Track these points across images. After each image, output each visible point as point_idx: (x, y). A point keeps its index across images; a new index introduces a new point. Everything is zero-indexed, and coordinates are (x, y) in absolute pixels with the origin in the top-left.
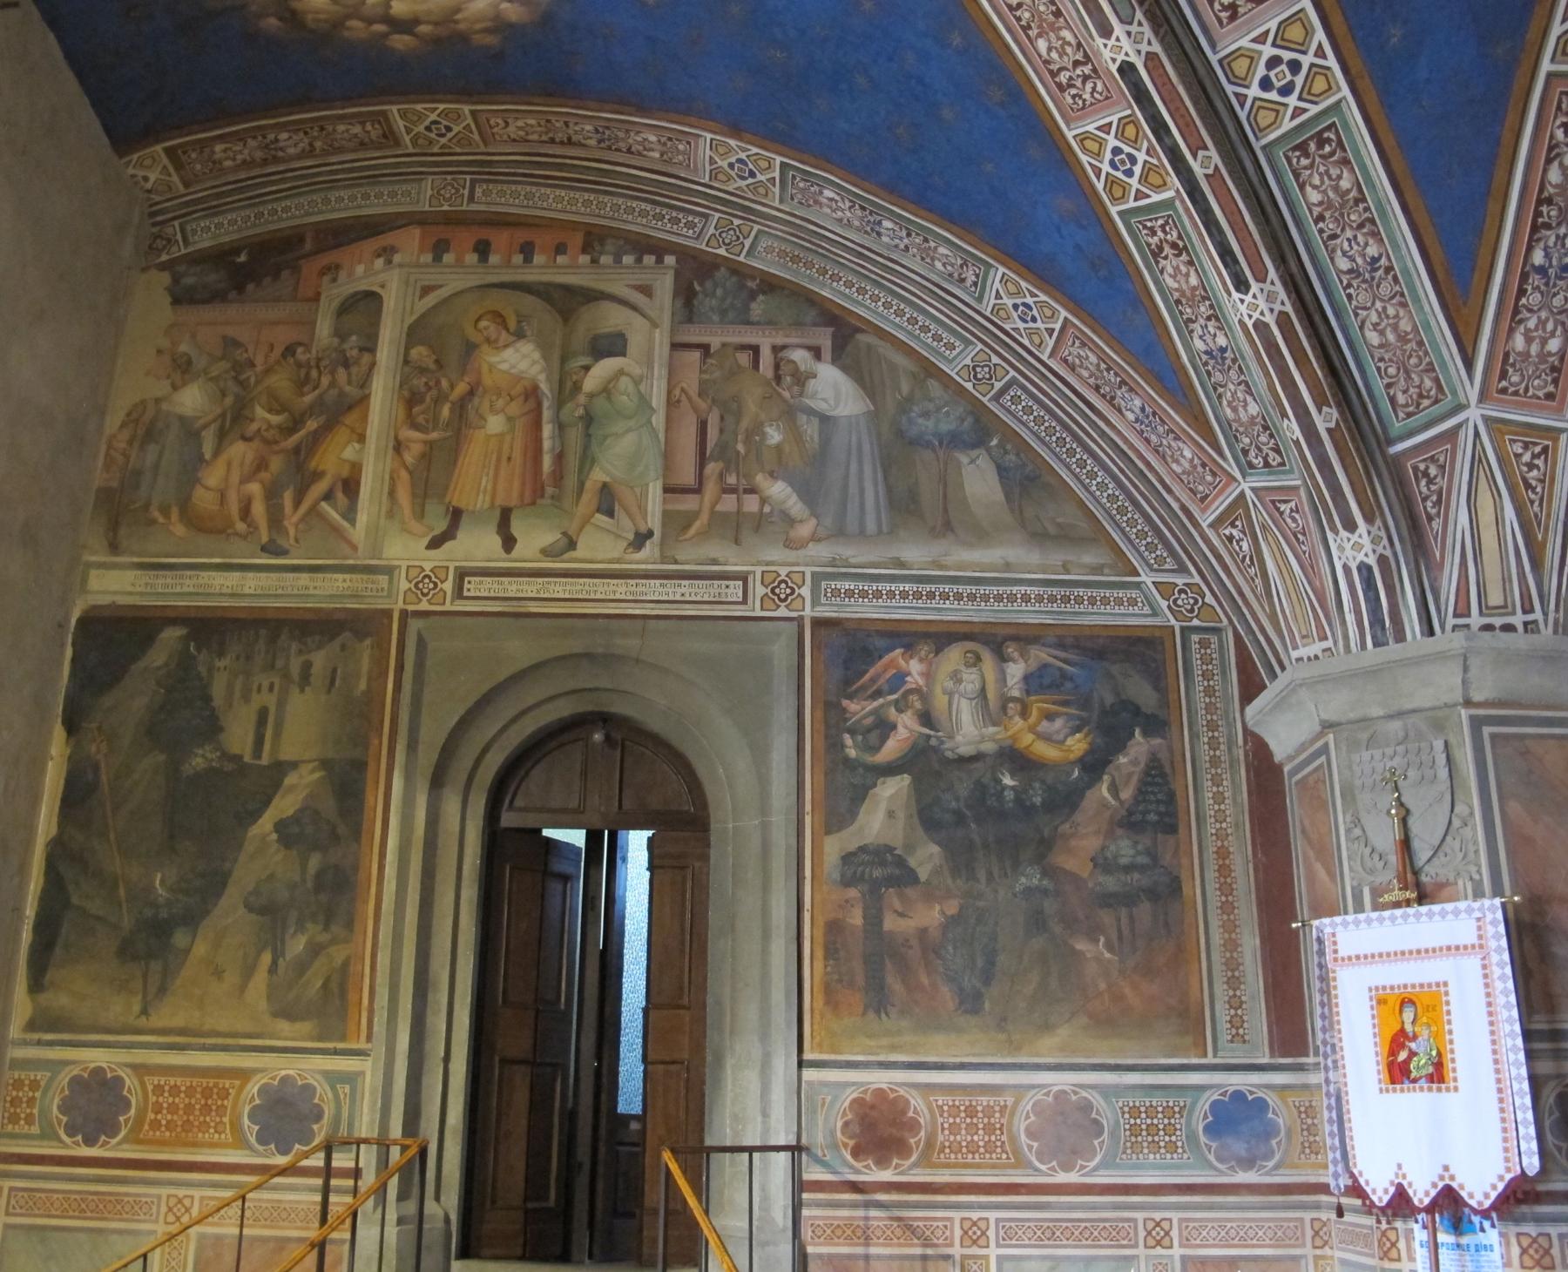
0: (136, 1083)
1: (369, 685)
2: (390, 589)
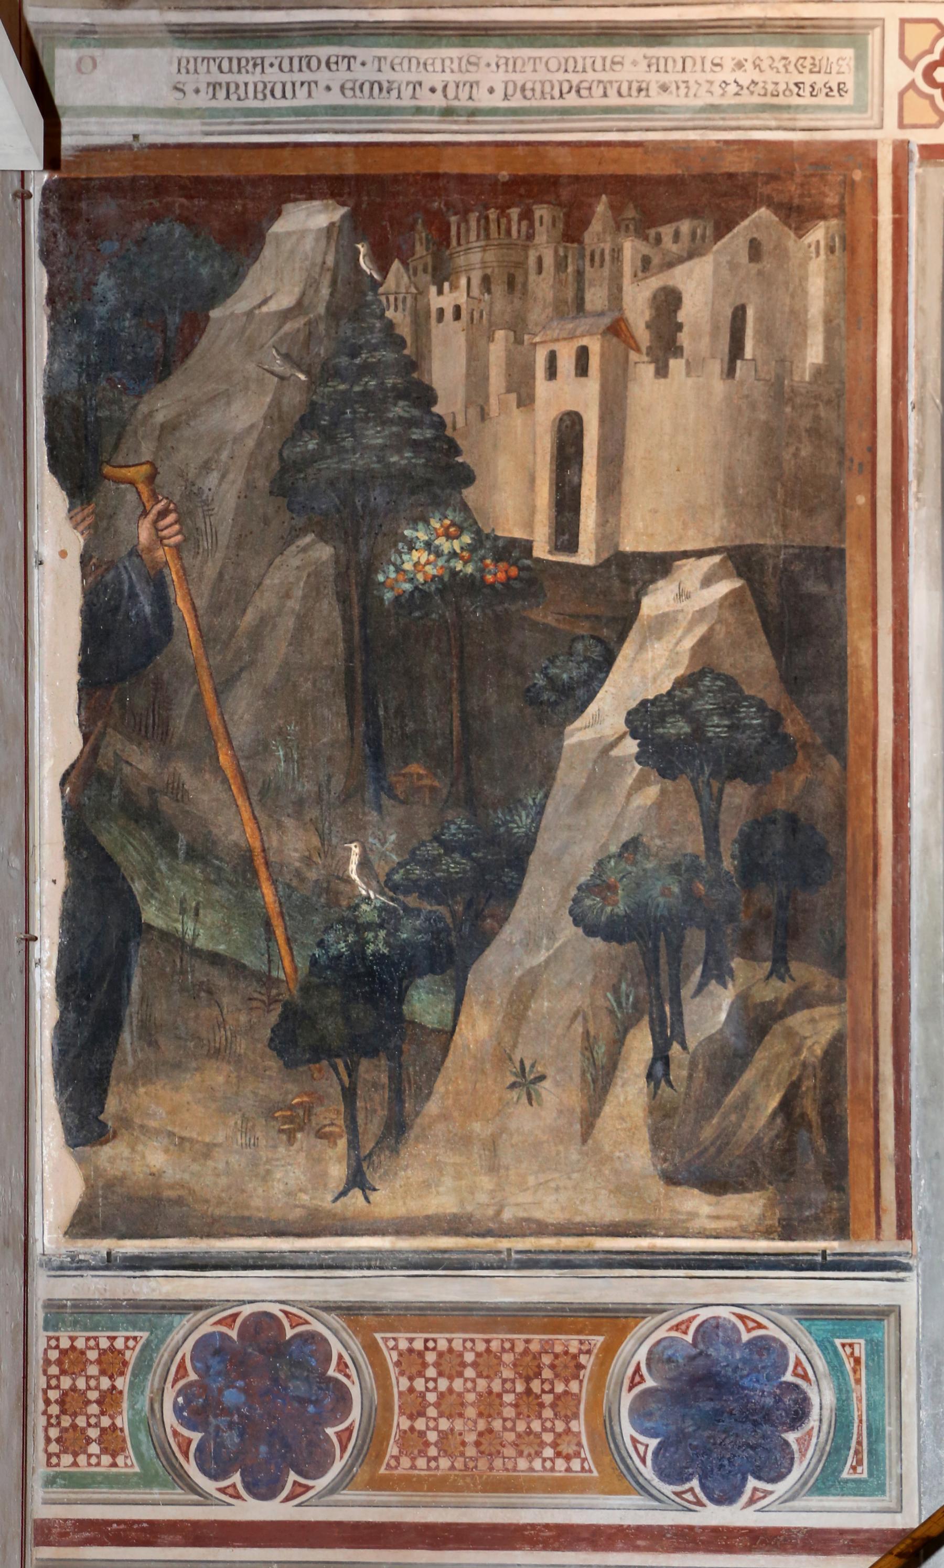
0: (355, 1345)
1: (828, 349)
2: (861, 86)
